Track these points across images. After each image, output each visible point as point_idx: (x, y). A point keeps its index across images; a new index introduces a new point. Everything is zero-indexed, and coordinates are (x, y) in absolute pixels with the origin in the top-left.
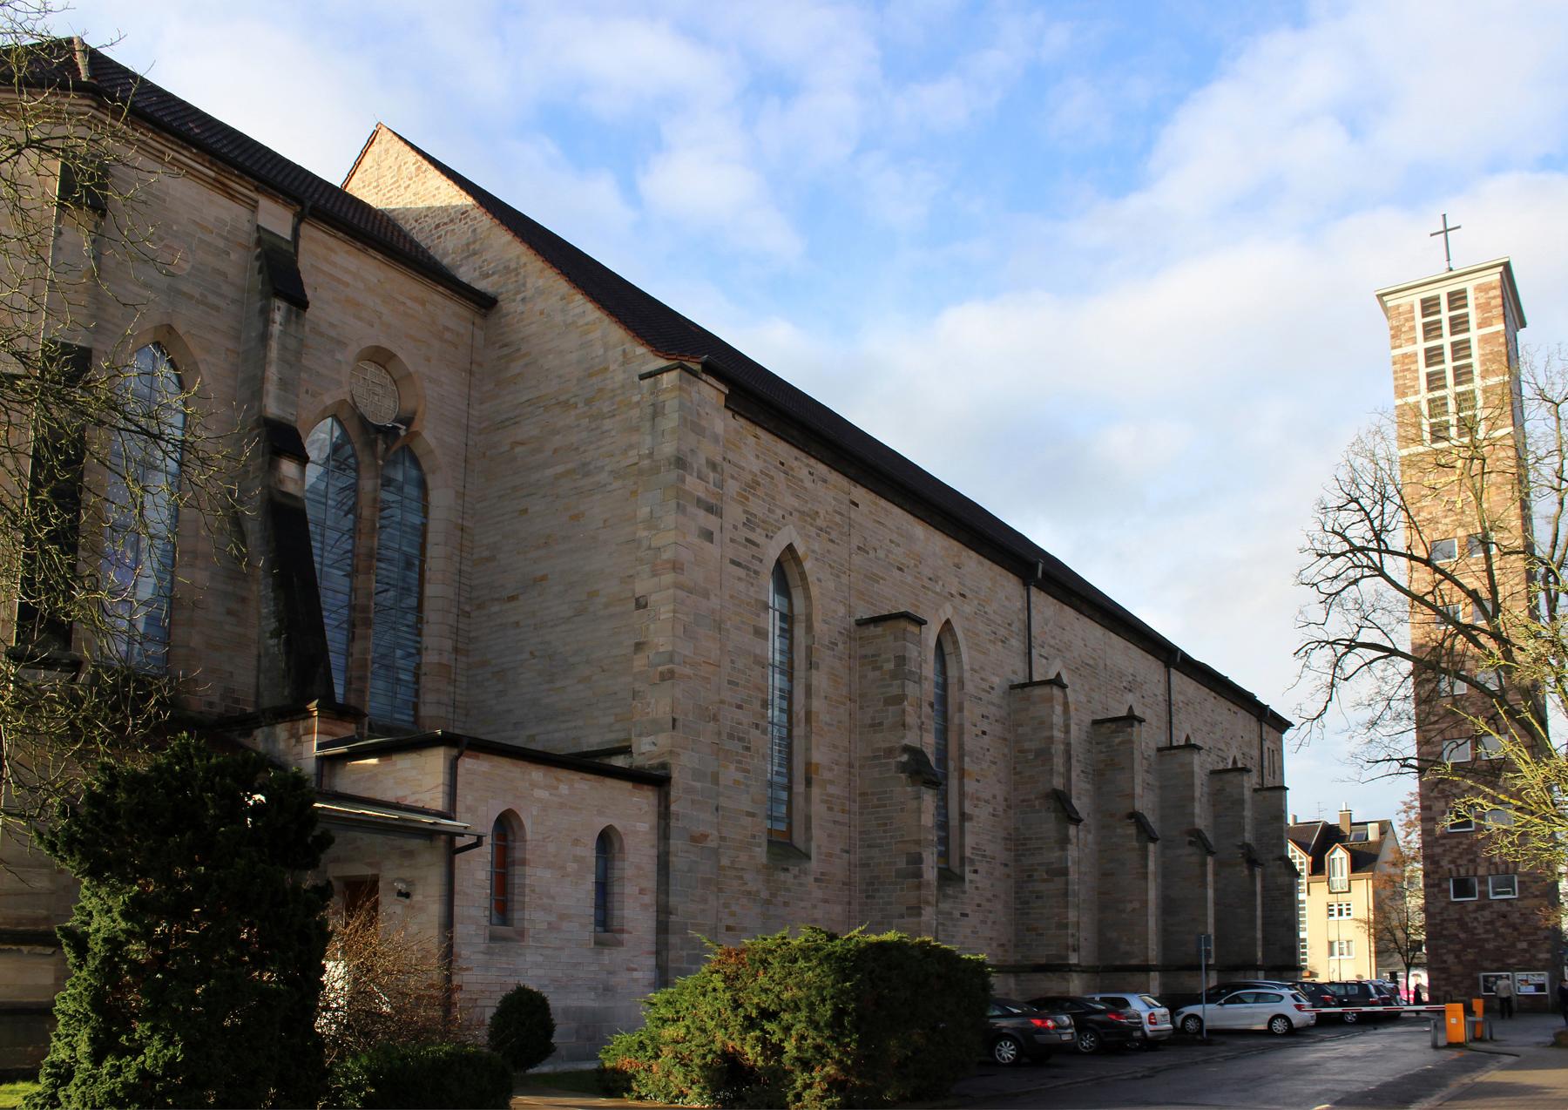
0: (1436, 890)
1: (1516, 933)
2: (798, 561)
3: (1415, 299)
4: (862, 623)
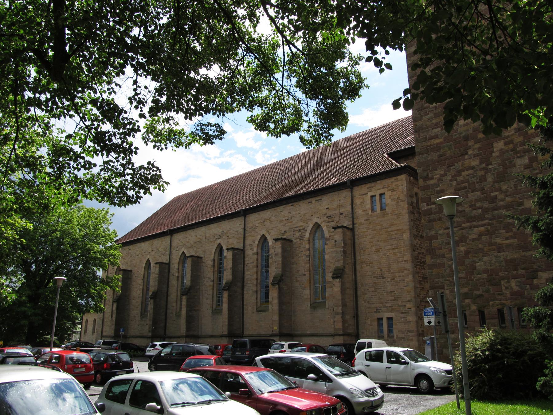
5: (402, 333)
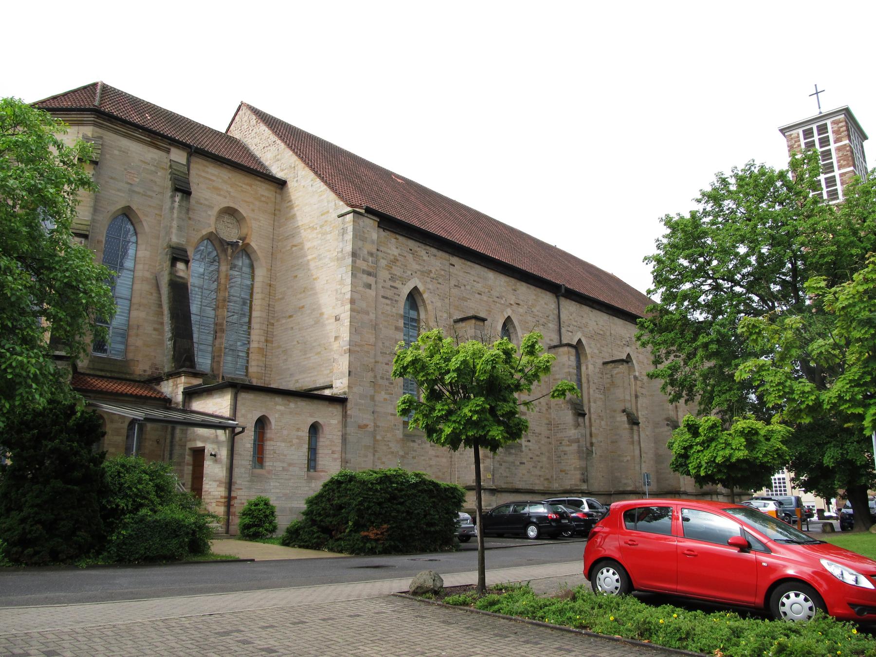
2: (420, 294)
4: (457, 321)
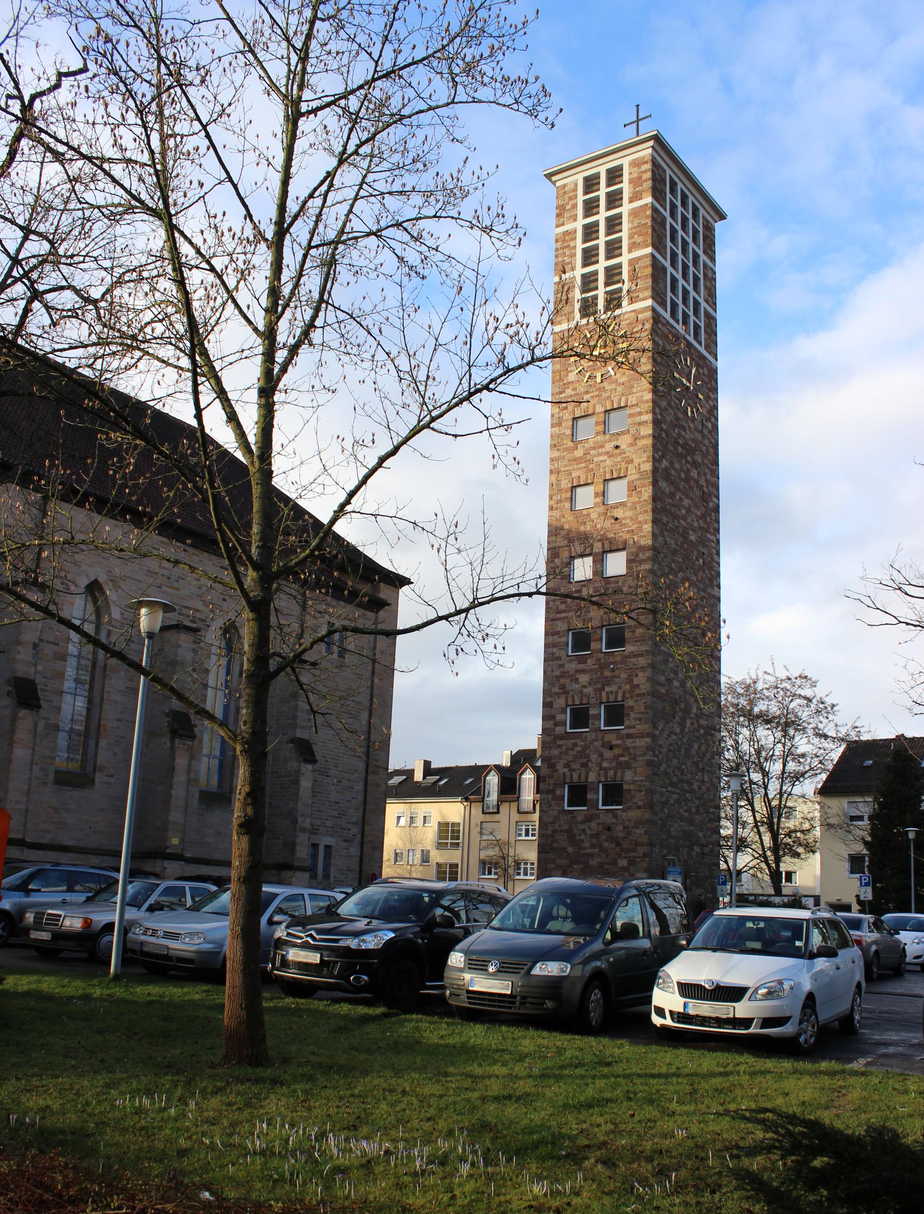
0: (550, 797)
1: (618, 848)
3: (578, 178)
5: (342, 874)
